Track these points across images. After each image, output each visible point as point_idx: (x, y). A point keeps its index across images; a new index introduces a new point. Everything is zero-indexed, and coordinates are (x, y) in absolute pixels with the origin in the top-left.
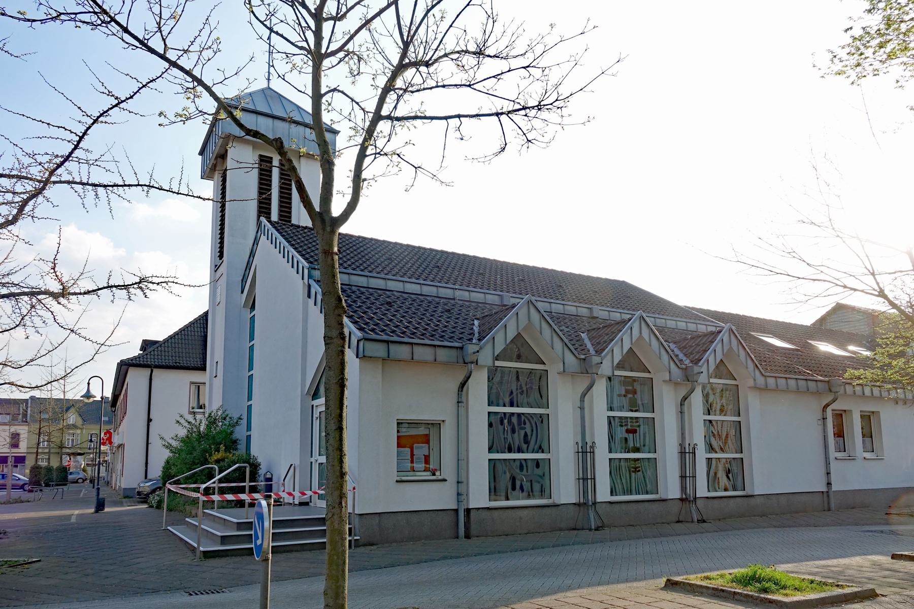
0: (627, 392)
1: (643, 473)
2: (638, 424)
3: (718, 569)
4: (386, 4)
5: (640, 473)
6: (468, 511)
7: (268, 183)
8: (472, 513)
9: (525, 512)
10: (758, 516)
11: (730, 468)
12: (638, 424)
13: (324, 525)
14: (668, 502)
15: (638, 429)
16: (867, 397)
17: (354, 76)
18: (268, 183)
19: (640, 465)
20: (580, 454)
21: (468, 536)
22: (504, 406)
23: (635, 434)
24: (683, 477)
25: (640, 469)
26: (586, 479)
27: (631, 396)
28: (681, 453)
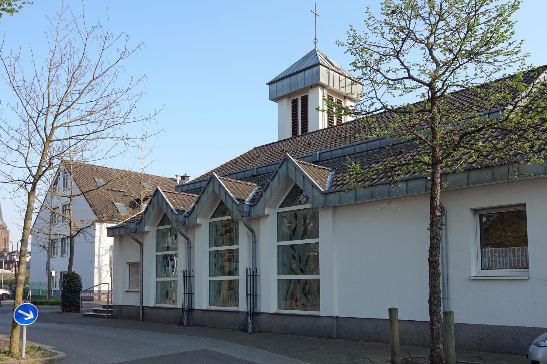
0: (226, 231)
1: (234, 291)
2: (233, 254)
3: (40, 343)
4: (54, 118)
5: (233, 291)
6: (143, 307)
7: (330, 123)
8: (145, 308)
9: (163, 311)
10: (324, 337)
11: (310, 289)
12: (233, 254)
13: (112, 309)
14: (240, 313)
15: (232, 258)
16: (232, 217)
17: (365, 44)
18: (330, 123)
19: (232, 285)
20: (249, 276)
21: (143, 320)
22: (165, 251)
23: (230, 262)
24: (255, 295)
25: (232, 288)
26: (189, 294)
27: (229, 234)
28: (257, 275)
